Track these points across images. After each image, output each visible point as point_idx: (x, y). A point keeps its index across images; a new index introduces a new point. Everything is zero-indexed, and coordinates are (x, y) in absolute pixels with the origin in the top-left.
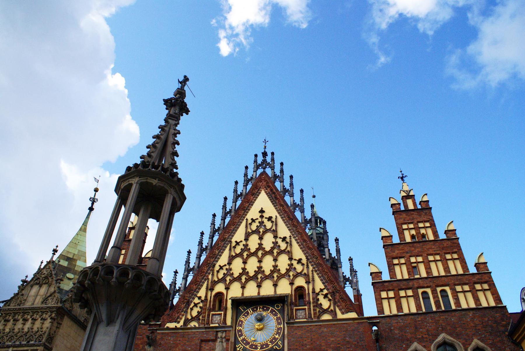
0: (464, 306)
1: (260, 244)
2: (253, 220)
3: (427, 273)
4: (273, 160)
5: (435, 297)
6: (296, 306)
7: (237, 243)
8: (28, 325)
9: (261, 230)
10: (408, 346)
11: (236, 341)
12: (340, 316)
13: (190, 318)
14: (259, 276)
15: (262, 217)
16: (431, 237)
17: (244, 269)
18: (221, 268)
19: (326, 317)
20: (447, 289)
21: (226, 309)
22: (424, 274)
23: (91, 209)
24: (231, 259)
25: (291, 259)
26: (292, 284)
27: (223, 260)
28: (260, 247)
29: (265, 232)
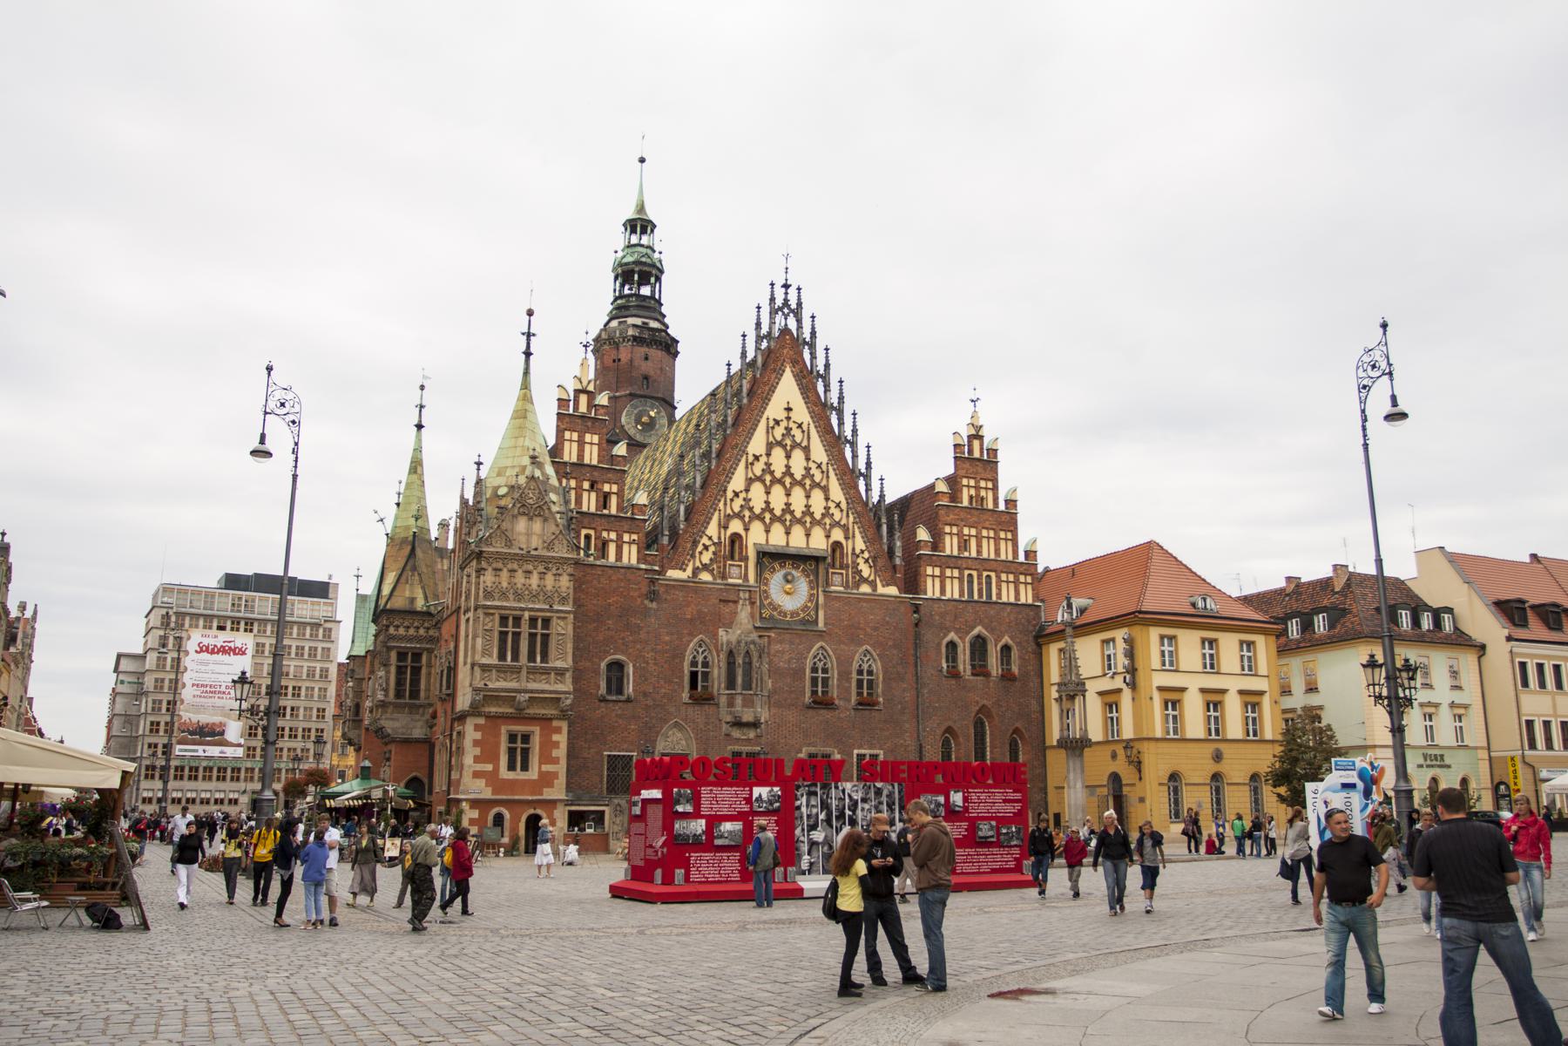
0: (1004, 599)
1: (788, 467)
2: (777, 422)
3: (979, 552)
4: (799, 304)
5: (980, 584)
6: (833, 567)
7: (757, 458)
8: (534, 581)
9: (788, 442)
10: (945, 635)
11: (762, 606)
12: (881, 590)
13: (698, 564)
14: (787, 518)
15: (788, 418)
16: (991, 506)
17: (767, 503)
18: (736, 494)
19: (865, 588)
20: (993, 575)
21: (746, 559)
22: (974, 554)
23: (528, 354)
24: (750, 482)
25: (827, 499)
26: (828, 537)
27: (737, 482)
28: (788, 472)
29: (793, 447)
